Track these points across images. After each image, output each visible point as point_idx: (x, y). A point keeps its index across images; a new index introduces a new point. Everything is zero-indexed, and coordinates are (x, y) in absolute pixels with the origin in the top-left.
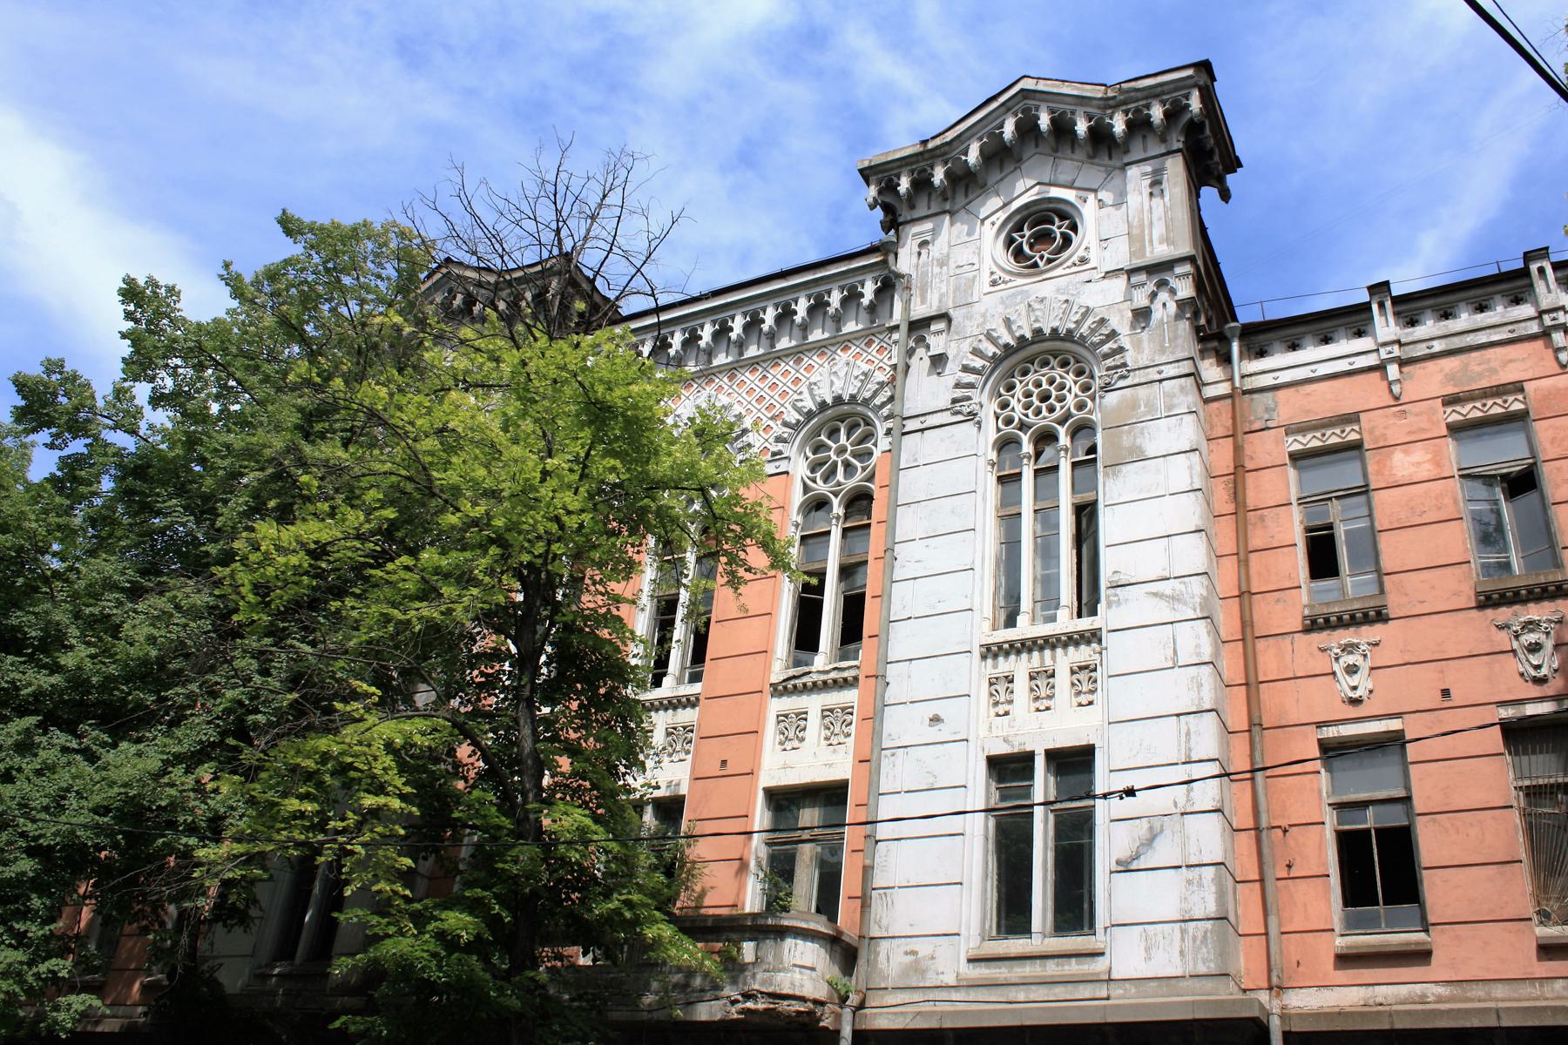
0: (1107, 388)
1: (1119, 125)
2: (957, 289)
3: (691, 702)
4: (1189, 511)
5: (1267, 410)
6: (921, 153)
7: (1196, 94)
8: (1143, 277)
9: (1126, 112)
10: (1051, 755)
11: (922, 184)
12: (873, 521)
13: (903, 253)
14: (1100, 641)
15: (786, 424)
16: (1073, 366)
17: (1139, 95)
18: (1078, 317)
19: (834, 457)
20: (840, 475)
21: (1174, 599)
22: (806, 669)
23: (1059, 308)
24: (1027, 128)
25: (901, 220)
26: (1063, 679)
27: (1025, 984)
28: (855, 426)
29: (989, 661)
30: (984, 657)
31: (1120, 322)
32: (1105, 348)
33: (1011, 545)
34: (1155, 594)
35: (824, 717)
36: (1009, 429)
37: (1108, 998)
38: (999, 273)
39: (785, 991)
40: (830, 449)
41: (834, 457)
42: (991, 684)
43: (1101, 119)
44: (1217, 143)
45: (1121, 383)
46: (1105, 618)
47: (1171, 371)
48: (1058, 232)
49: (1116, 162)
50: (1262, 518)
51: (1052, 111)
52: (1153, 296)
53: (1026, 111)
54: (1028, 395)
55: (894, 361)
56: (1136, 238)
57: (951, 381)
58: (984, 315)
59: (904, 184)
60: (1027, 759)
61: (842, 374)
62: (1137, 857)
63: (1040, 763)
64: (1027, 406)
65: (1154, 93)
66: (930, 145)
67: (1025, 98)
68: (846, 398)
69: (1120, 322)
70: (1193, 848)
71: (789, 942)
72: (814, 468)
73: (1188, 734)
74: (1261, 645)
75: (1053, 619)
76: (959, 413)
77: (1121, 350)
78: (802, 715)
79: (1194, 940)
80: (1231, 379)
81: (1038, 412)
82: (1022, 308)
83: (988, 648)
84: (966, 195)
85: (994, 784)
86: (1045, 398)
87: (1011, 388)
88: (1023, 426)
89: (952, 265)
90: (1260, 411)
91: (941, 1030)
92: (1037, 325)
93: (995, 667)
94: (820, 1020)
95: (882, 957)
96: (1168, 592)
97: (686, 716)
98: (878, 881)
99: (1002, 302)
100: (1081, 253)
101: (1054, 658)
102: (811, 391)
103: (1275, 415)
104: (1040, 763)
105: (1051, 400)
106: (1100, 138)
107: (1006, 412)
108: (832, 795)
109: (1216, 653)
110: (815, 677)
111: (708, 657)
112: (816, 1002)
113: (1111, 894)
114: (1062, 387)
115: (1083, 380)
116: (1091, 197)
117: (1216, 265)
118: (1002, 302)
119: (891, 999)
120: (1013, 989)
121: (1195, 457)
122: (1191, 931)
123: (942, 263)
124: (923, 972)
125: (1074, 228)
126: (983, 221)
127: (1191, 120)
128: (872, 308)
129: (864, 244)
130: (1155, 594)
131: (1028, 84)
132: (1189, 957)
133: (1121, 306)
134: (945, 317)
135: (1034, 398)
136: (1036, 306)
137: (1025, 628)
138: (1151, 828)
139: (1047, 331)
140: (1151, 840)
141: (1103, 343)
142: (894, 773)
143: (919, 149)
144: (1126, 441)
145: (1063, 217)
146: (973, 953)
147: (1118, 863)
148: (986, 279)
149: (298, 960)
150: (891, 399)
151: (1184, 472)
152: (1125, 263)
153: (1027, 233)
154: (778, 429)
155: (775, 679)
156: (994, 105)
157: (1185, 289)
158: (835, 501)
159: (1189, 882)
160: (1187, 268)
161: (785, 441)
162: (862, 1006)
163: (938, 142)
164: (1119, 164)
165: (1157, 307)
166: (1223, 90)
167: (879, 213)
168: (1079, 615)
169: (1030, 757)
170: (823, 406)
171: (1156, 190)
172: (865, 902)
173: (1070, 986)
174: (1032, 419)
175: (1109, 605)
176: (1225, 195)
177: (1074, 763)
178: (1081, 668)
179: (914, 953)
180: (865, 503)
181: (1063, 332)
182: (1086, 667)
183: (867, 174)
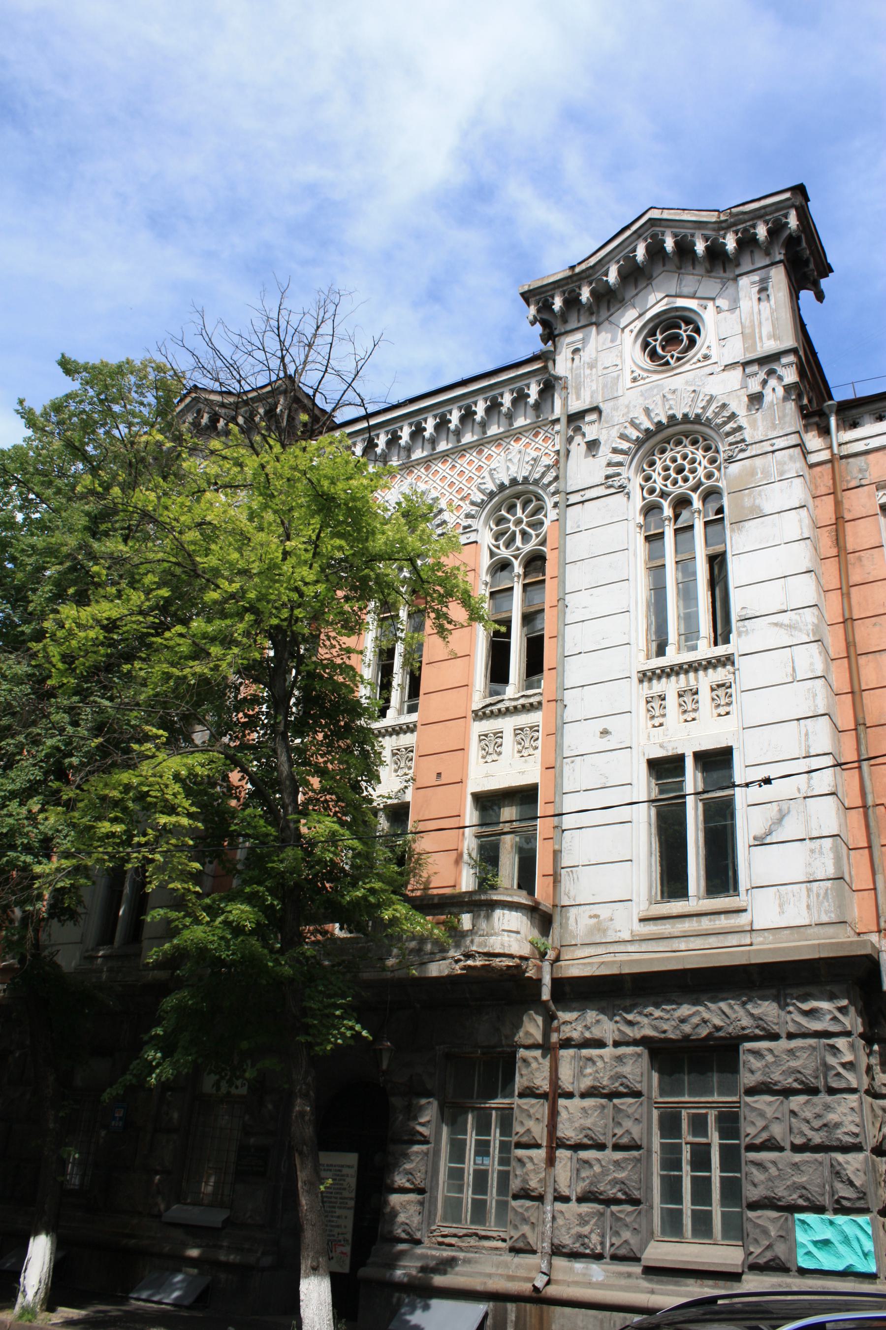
0: (730, 460)
2: (605, 386)
3: (410, 729)
4: (801, 556)
5: (861, 471)
6: (570, 277)
7: (793, 214)
8: (755, 368)
9: (736, 232)
11: (572, 302)
12: (547, 577)
13: (559, 359)
14: (733, 664)
15: (473, 503)
16: (701, 444)
17: (746, 217)
18: (704, 404)
19: (513, 528)
20: (519, 541)
21: (791, 627)
22: (500, 698)
23: (688, 398)
24: (656, 251)
25: (556, 332)
26: (705, 695)
29: (646, 684)
30: (641, 681)
31: (739, 405)
32: (727, 428)
33: (658, 590)
34: (776, 624)
35: (516, 735)
37: (751, 945)
38: (638, 372)
39: (497, 951)
40: (509, 521)
41: (513, 528)
42: (648, 702)
43: (715, 241)
44: (812, 253)
45: (742, 456)
46: (736, 645)
48: (684, 335)
49: (731, 275)
50: (860, 559)
51: (675, 235)
52: (764, 383)
53: (654, 236)
54: (666, 469)
55: (557, 447)
56: (748, 336)
58: (628, 407)
59: (558, 303)
60: (679, 759)
61: (516, 460)
62: (770, 833)
63: (689, 763)
64: (666, 479)
66: (577, 270)
67: (653, 226)
68: (520, 479)
69: (739, 405)
71: (498, 913)
73: (807, 734)
74: (862, 660)
75: (694, 648)
76: (611, 486)
77: (740, 428)
78: (499, 734)
79: (818, 895)
80: (830, 447)
81: (675, 482)
82: (658, 399)
83: (644, 673)
84: (609, 309)
85: (653, 781)
86: (680, 470)
87: (652, 464)
88: (663, 495)
89: (600, 367)
90: (855, 472)
91: (621, 975)
92: (671, 412)
93: (650, 688)
94: (525, 971)
95: (572, 921)
96: (786, 622)
97: (407, 740)
99: (642, 395)
100: (704, 351)
101: (697, 679)
102: (491, 475)
103: (867, 475)
104: (689, 763)
105: (686, 473)
106: (716, 254)
107: (650, 484)
108: (526, 796)
109: (827, 668)
110: (507, 704)
111: (422, 692)
112: (522, 958)
113: (750, 863)
114: (693, 461)
115: (710, 454)
116: (710, 304)
117: (814, 354)
118: (642, 395)
121: (803, 512)
122: (815, 889)
123: (592, 366)
124: (605, 931)
125: (697, 331)
126: (623, 329)
127: (790, 235)
128: (537, 406)
129: (525, 353)
130: (776, 624)
131: (655, 214)
132: (814, 910)
133: (739, 393)
134: (596, 409)
135: (671, 472)
136: (669, 396)
137: (673, 656)
138: (780, 810)
139: (679, 416)
140: (780, 820)
141: (725, 423)
142: (575, 776)
143: (568, 273)
144: (747, 502)
145: (688, 322)
146: (643, 915)
147: (755, 838)
148: (628, 377)
150: (556, 478)
151: (796, 525)
152: (741, 358)
153: (659, 337)
154: (467, 508)
155: (475, 708)
156: (628, 233)
157: (790, 376)
158: (516, 563)
159: (812, 851)
160: (791, 358)
161: (473, 517)
162: (557, 959)
163: (583, 266)
164: (732, 276)
165: (768, 391)
166: (814, 207)
167: (538, 328)
168: (716, 644)
169: (681, 758)
170: (502, 487)
171: (763, 296)
172: (556, 878)
173: (721, 937)
174: (670, 488)
175: (739, 634)
176: (820, 296)
177: (716, 761)
178: (719, 686)
179: (596, 916)
180: (539, 563)
181: (692, 416)
182: (723, 685)
183: (527, 296)
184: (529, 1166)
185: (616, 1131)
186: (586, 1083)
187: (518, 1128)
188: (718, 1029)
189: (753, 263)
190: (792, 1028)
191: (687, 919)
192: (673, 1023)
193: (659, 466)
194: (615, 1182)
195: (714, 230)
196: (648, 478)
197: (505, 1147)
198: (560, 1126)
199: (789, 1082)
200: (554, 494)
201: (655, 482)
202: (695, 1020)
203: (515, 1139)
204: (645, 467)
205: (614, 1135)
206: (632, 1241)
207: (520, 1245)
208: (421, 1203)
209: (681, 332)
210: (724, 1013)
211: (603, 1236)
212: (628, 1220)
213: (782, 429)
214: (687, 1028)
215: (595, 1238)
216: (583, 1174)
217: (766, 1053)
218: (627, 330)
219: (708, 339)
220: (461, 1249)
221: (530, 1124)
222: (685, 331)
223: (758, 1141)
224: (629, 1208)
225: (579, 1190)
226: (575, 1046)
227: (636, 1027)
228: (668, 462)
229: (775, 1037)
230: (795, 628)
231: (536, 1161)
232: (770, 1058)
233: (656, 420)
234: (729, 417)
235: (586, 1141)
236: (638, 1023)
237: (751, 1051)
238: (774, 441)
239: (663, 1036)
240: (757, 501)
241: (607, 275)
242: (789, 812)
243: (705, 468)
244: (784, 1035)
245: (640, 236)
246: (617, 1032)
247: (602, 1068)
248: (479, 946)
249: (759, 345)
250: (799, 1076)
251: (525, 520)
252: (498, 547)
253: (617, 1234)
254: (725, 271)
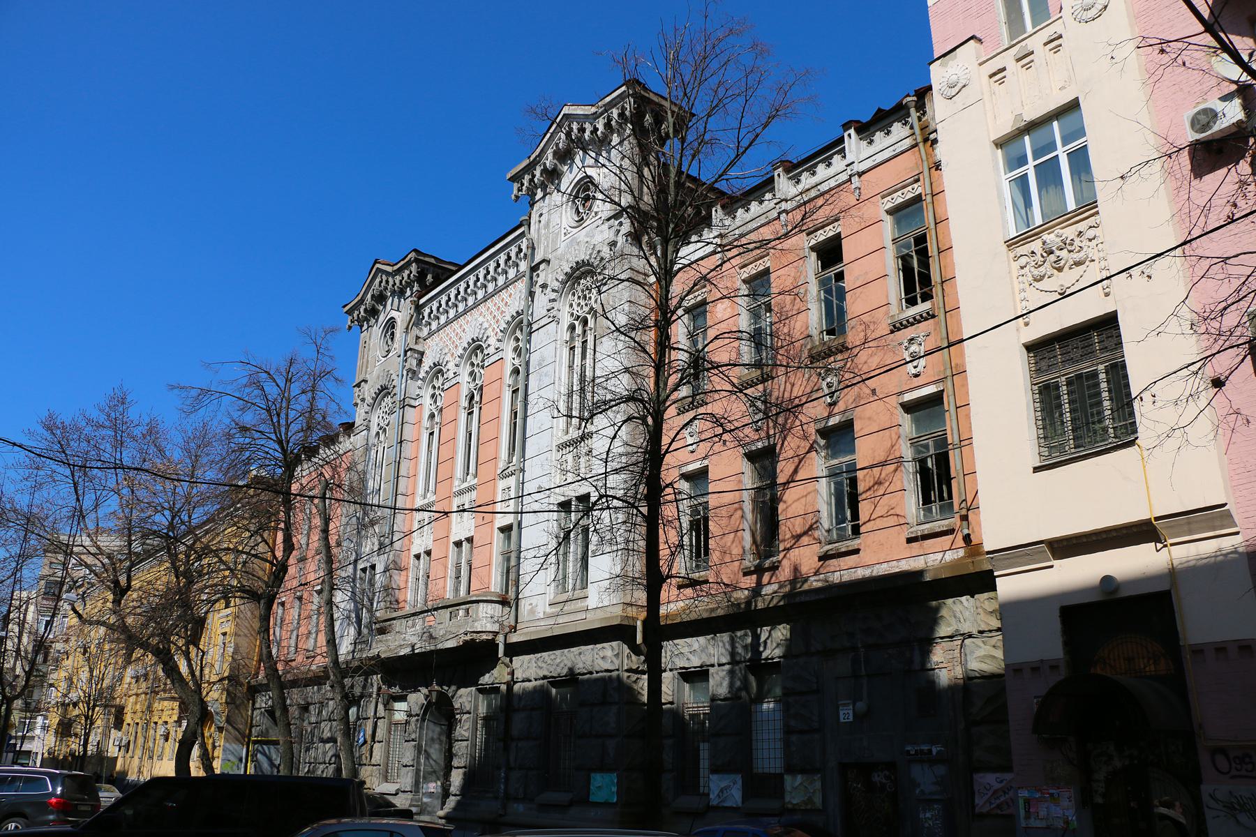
52: (619, 231)
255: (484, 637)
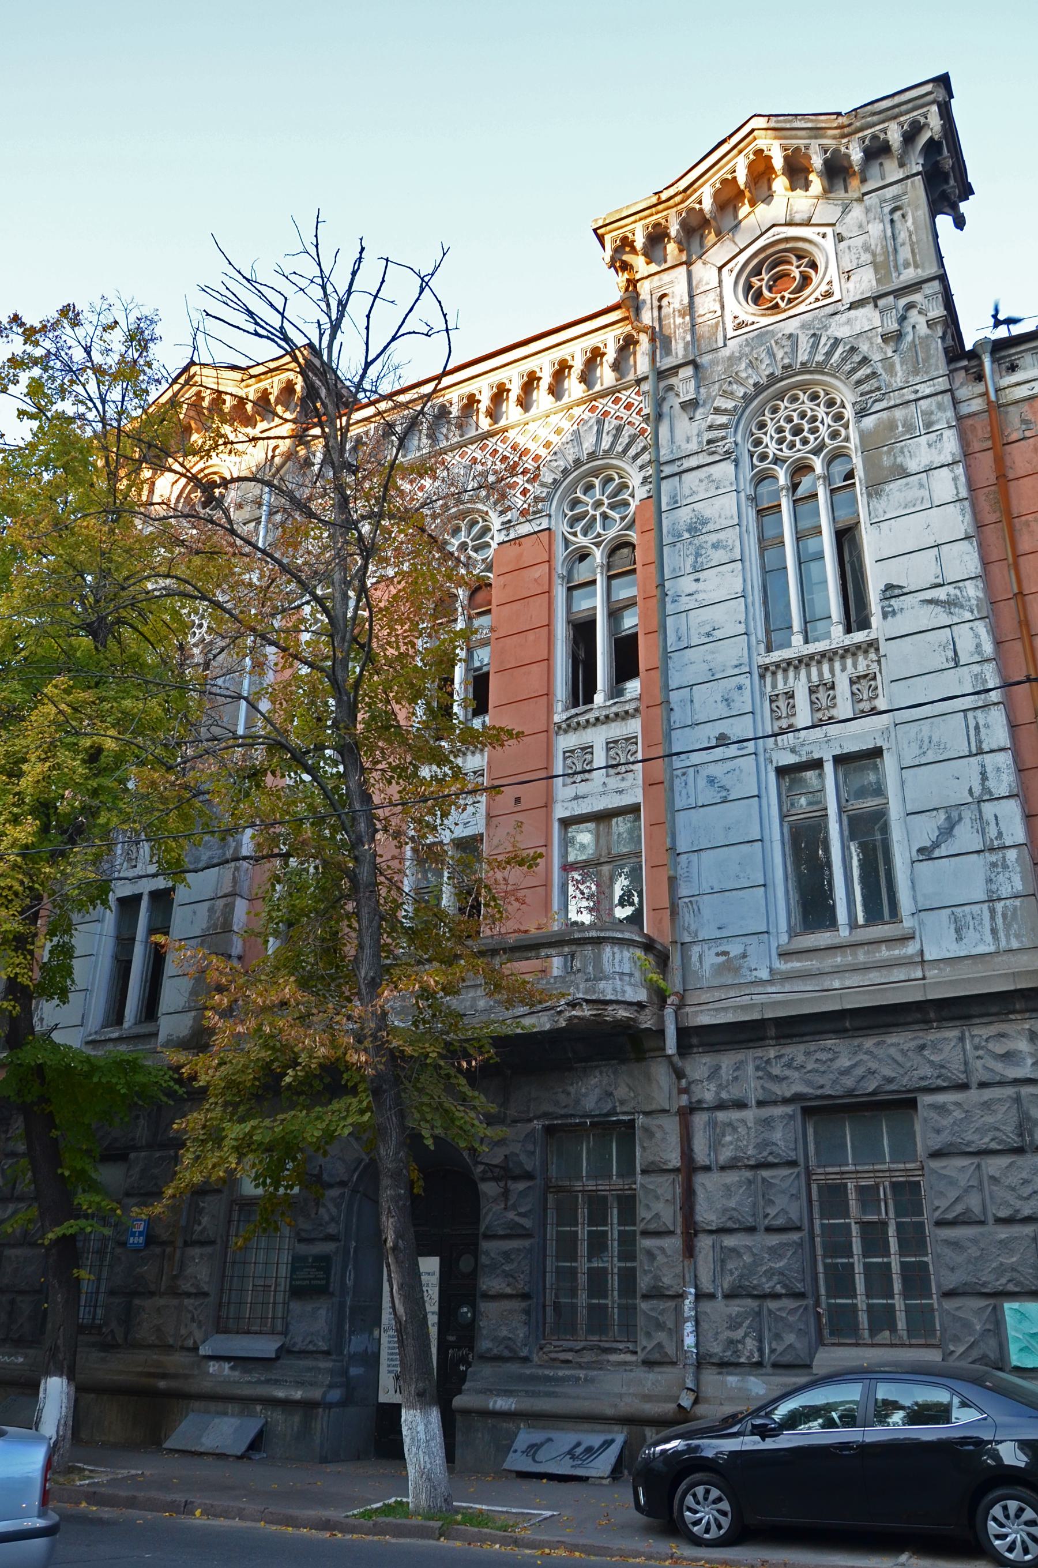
0: (861, 413)
1: (856, 155)
4: (955, 521)
7: (934, 108)
10: (838, 760)
12: (638, 566)
14: (877, 649)
17: (875, 118)
20: (599, 528)
21: (949, 604)
27: (837, 972)
28: (609, 480)
33: (771, 574)
34: (930, 602)
35: (608, 749)
36: (764, 465)
37: (924, 978)
41: (592, 512)
42: (771, 701)
43: (836, 151)
47: (926, 389)
50: (1027, 524)
52: (902, 319)
54: (780, 430)
55: (645, 412)
56: (882, 266)
57: (704, 425)
62: (936, 845)
63: (829, 767)
64: (780, 441)
65: (890, 115)
66: (664, 196)
70: (993, 832)
71: (608, 950)
72: (574, 521)
73: (977, 728)
76: (714, 453)
77: (874, 373)
80: (986, 394)
84: (702, 246)
86: (797, 431)
87: (762, 426)
95: (695, 958)
96: (943, 598)
98: (683, 891)
100: (824, 288)
101: (832, 671)
105: (805, 434)
107: (760, 449)
111: (490, 706)
112: (640, 1006)
114: (814, 419)
115: (834, 410)
116: (829, 230)
118: (748, 344)
119: (705, 997)
120: (828, 978)
124: (737, 970)
125: (814, 266)
126: (720, 269)
127: (931, 139)
132: (1002, 934)
135: (787, 434)
137: (797, 646)
138: (948, 818)
140: (947, 831)
141: (854, 371)
144: (886, 461)
149: (126, 1025)
151: (946, 485)
159: (994, 865)
161: (543, 500)
168: (848, 630)
171: (897, 215)
173: (884, 971)
174: (787, 453)
175: (885, 615)
176: (960, 223)
179: (725, 953)
182: (866, 676)
184: (661, 1259)
185: (768, 1210)
186: (725, 1155)
187: (642, 1213)
188: (890, 1080)
189: (883, 178)
190: (986, 1077)
191: (838, 951)
192: (831, 1076)
193: (771, 428)
194: (770, 1273)
195: (834, 138)
196: (758, 443)
197: (627, 1240)
198: (698, 1208)
199: (985, 1142)
200: (642, 468)
201: (767, 446)
202: (860, 1071)
203: (640, 1227)
204: (754, 431)
205: (766, 1216)
206: (798, 1345)
207: (656, 1357)
208: (527, 1312)
209: (793, 268)
210: (896, 1061)
211: (760, 1341)
212: (791, 1319)
213: (927, 373)
214: (849, 1082)
215: (750, 1344)
216: (730, 1266)
217: (952, 1108)
218: (725, 270)
219: (829, 275)
220: (580, 1366)
221: (659, 1207)
222: (798, 267)
223: (950, 1216)
224: (790, 1304)
225: (726, 1286)
226: (708, 1109)
227: (784, 1084)
228: (782, 423)
229: (964, 1087)
230: (955, 605)
231: (669, 1253)
232: (958, 1114)
233: (767, 373)
234: (859, 363)
235: (730, 1224)
236: (786, 1078)
237: (934, 1107)
238: (917, 387)
239: (819, 1092)
240: (899, 460)
241: (700, 203)
242: (960, 819)
243: (829, 426)
244: (974, 1085)
245: (740, 152)
246: (760, 1091)
247: (742, 1133)
248: (585, 993)
249: (894, 275)
250: (998, 1134)
251: (606, 502)
252: (575, 534)
253: (778, 1337)
254: (846, 191)
255: (622, 1013)
